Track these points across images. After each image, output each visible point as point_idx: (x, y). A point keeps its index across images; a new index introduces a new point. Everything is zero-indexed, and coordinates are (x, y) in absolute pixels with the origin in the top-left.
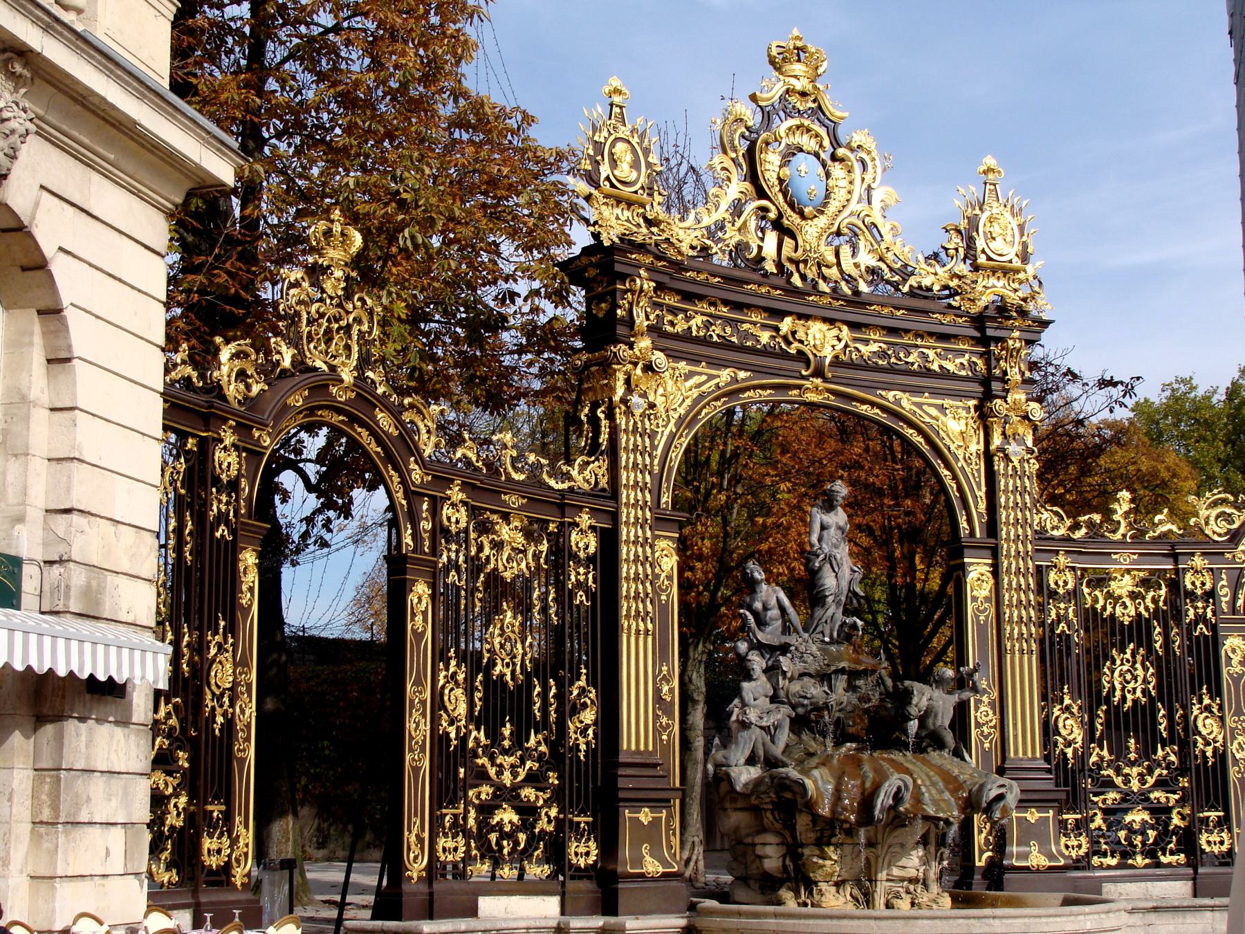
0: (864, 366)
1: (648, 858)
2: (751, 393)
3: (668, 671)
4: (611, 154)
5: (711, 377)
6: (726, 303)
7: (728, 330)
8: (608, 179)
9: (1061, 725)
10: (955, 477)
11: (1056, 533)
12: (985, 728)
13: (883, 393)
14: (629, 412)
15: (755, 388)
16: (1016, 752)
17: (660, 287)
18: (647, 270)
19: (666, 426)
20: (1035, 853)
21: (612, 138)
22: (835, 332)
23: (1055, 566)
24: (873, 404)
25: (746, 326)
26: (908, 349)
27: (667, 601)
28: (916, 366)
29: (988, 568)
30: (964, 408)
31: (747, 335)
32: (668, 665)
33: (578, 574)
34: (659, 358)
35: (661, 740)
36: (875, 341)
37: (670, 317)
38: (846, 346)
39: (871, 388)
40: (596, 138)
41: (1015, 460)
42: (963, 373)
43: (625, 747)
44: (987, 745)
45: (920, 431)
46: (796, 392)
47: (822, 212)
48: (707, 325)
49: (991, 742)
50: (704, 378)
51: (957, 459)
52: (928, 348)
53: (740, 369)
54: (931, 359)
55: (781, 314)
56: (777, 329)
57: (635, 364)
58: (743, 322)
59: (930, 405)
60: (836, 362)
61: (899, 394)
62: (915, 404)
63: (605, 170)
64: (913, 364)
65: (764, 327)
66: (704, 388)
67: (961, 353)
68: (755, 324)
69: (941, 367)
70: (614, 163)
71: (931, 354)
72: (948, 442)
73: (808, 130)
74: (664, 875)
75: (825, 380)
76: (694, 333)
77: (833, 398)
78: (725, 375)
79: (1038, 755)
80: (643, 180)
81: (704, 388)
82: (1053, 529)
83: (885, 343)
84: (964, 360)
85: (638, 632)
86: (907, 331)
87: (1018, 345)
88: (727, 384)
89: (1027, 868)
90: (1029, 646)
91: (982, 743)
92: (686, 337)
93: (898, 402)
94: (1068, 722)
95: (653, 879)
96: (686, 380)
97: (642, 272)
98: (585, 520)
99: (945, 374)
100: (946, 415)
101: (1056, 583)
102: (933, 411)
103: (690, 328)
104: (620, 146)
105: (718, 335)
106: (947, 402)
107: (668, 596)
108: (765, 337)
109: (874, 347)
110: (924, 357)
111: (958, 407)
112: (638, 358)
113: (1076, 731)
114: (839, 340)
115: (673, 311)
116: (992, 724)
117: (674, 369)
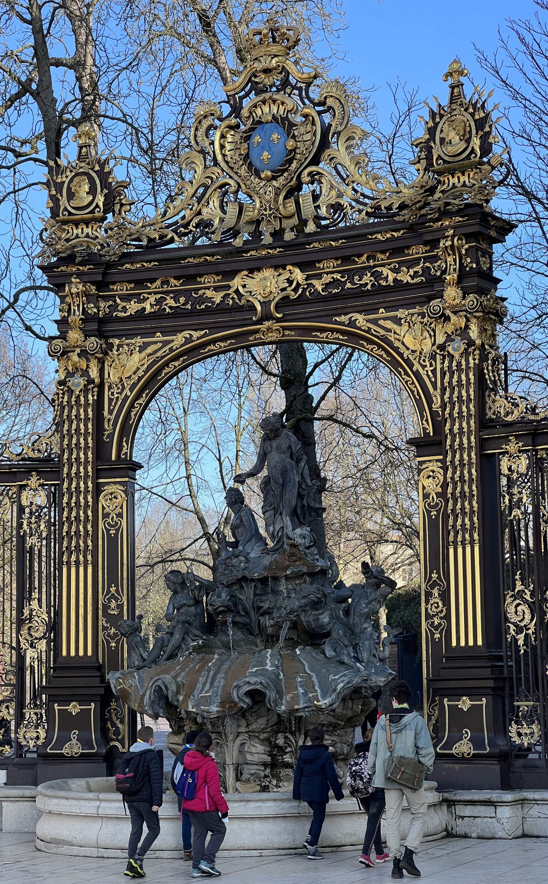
0: (317, 298)
1: (74, 741)
2: (212, 347)
3: (117, 591)
4: (69, 188)
5: (165, 343)
6: (177, 278)
7: (182, 300)
8: (66, 209)
9: (511, 609)
10: (413, 383)
11: (509, 419)
12: (436, 621)
13: (337, 319)
14: (71, 392)
15: (214, 341)
16: (458, 639)
17: (101, 285)
18: (79, 275)
19: (121, 393)
20: (465, 741)
21: (73, 174)
22: (287, 275)
23: (507, 452)
24: (332, 330)
25: (201, 292)
26: (361, 272)
27: (116, 535)
28: (369, 287)
29: (440, 465)
30: (419, 314)
31: (203, 300)
32: (117, 586)
33: (30, 523)
34: (93, 342)
35: (110, 648)
36: (327, 273)
37: (124, 304)
38: (298, 285)
39: (328, 317)
40: (59, 180)
41: (457, 356)
42: (415, 280)
43: (64, 653)
44: (437, 636)
45: (379, 346)
46: (258, 336)
47: (286, 170)
48: (159, 302)
49: (441, 633)
50: (160, 345)
51: (411, 365)
52: (383, 265)
53: (196, 330)
54: (385, 273)
55: (232, 274)
56: (229, 287)
57: (74, 351)
58: (196, 290)
59: (385, 319)
60: (284, 303)
61: (356, 316)
62: (367, 321)
63: (64, 202)
64: (367, 284)
65: (217, 289)
66: (159, 354)
67: (416, 262)
68: (208, 288)
69: (395, 280)
70: (71, 196)
71: (385, 271)
72: (402, 349)
73: (274, 101)
74: (83, 756)
75: (278, 320)
76: (148, 309)
77: (293, 333)
78: (179, 339)
79: (480, 643)
80: (100, 200)
81: (159, 354)
82: (507, 414)
83: (338, 272)
84: (418, 268)
85: (77, 563)
86: (360, 256)
87: (449, 243)
88: (182, 346)
89: (452, 755)
90: (471, 536)
91: (433, 634)
92: (140, 315)
93: (352, 323)
94: (519, 608)
95: (72, 758)
96: (140, 352)
97: (73, 280)
98: (34, 481)
99: (398, 285)
100: (401, 325)
101: (510, 469)
102: (389, 324)
103: (144, 309)
104: (76, 179)
105: (170, 307)
106: (401, 313)
107: (117, 530)
108: (218, 298)
109: (327, 279)
110: (377, 276)
111: (413, 315)
112: (74, 347)
113: (528, 616)
114: (290, 282)
115: (126, 298)
116: (442, 615)
117: (128, 345)
